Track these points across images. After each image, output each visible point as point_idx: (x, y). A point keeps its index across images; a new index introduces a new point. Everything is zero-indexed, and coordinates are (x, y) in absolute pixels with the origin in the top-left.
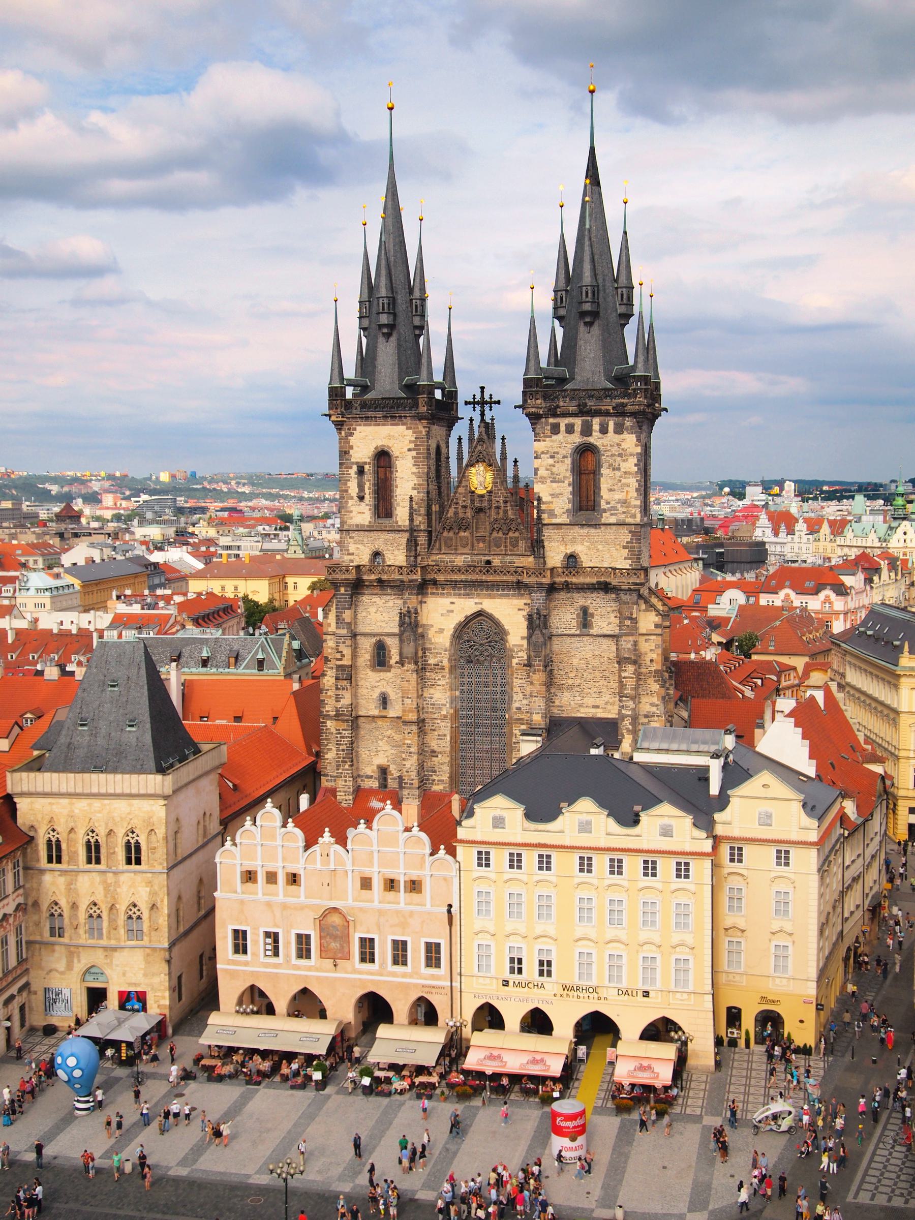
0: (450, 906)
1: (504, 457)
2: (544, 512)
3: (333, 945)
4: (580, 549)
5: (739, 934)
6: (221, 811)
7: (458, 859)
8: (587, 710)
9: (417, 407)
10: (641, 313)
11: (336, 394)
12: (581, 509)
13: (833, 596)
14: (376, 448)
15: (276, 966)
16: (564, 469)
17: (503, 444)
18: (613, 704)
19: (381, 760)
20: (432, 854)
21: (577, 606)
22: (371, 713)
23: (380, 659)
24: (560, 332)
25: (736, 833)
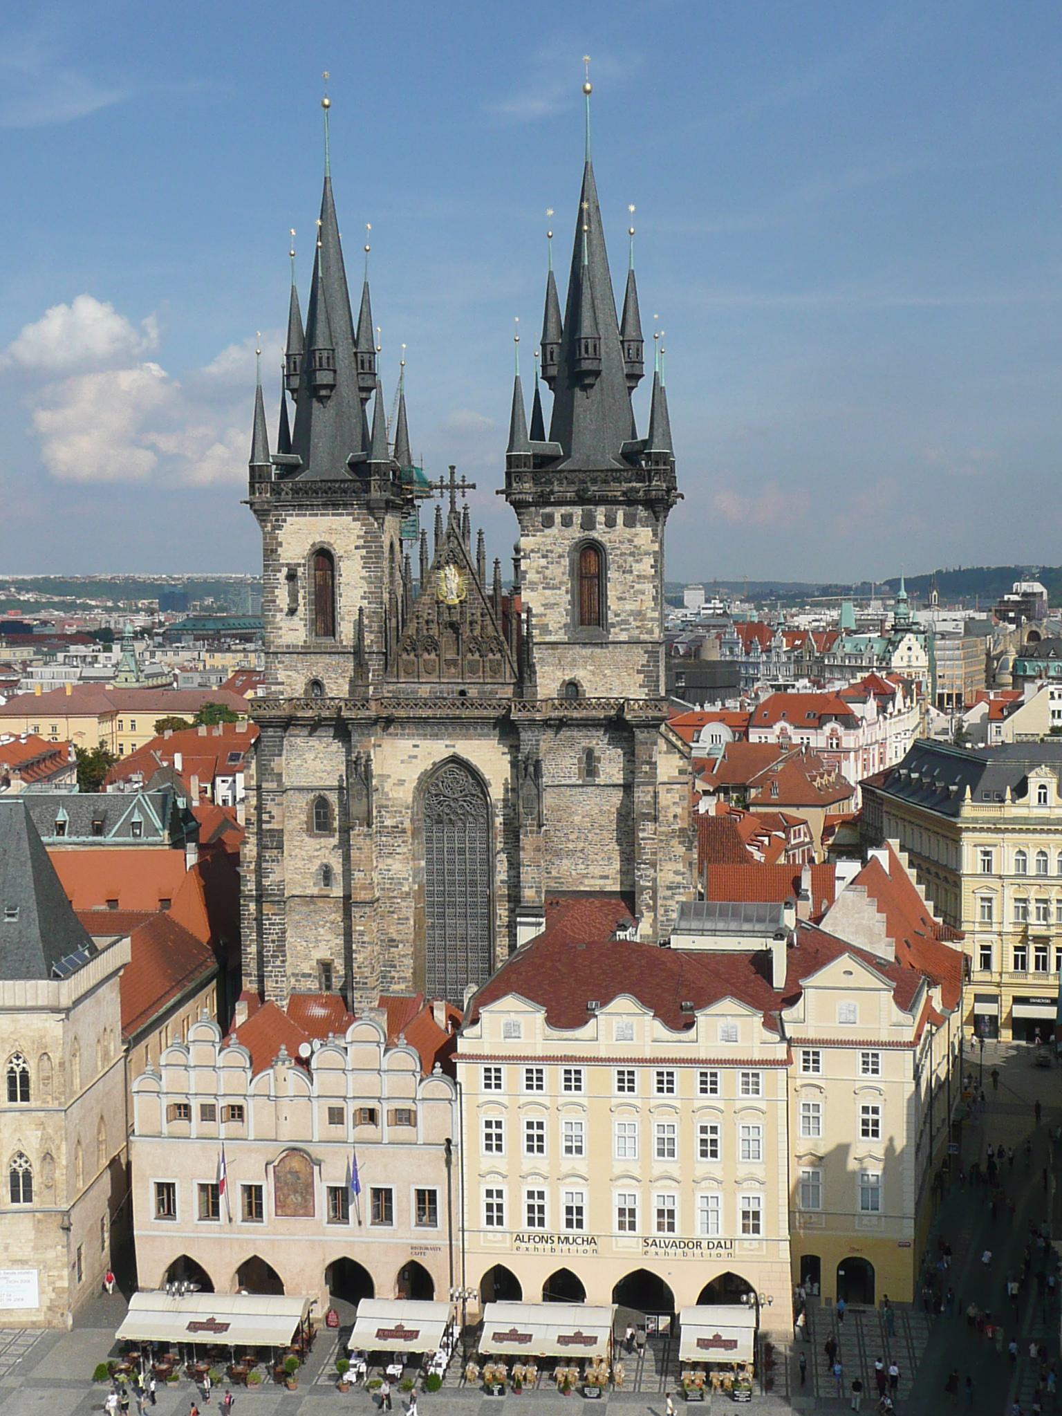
1: (480, 557)
2: (535, 627)
3: (295, 1199)
7: (459, 1079)
8: (592, 882)
9: (368, 491)
11: (257, 475)
12: (582, 624)
13: (841, 730)
14: (313, 545)
16: (560, 571)
17: (480, 540)
19: (323, 953)
21: (580, 747)
22: (308, 892)
23: (320, 820)
25: (811, 1034)
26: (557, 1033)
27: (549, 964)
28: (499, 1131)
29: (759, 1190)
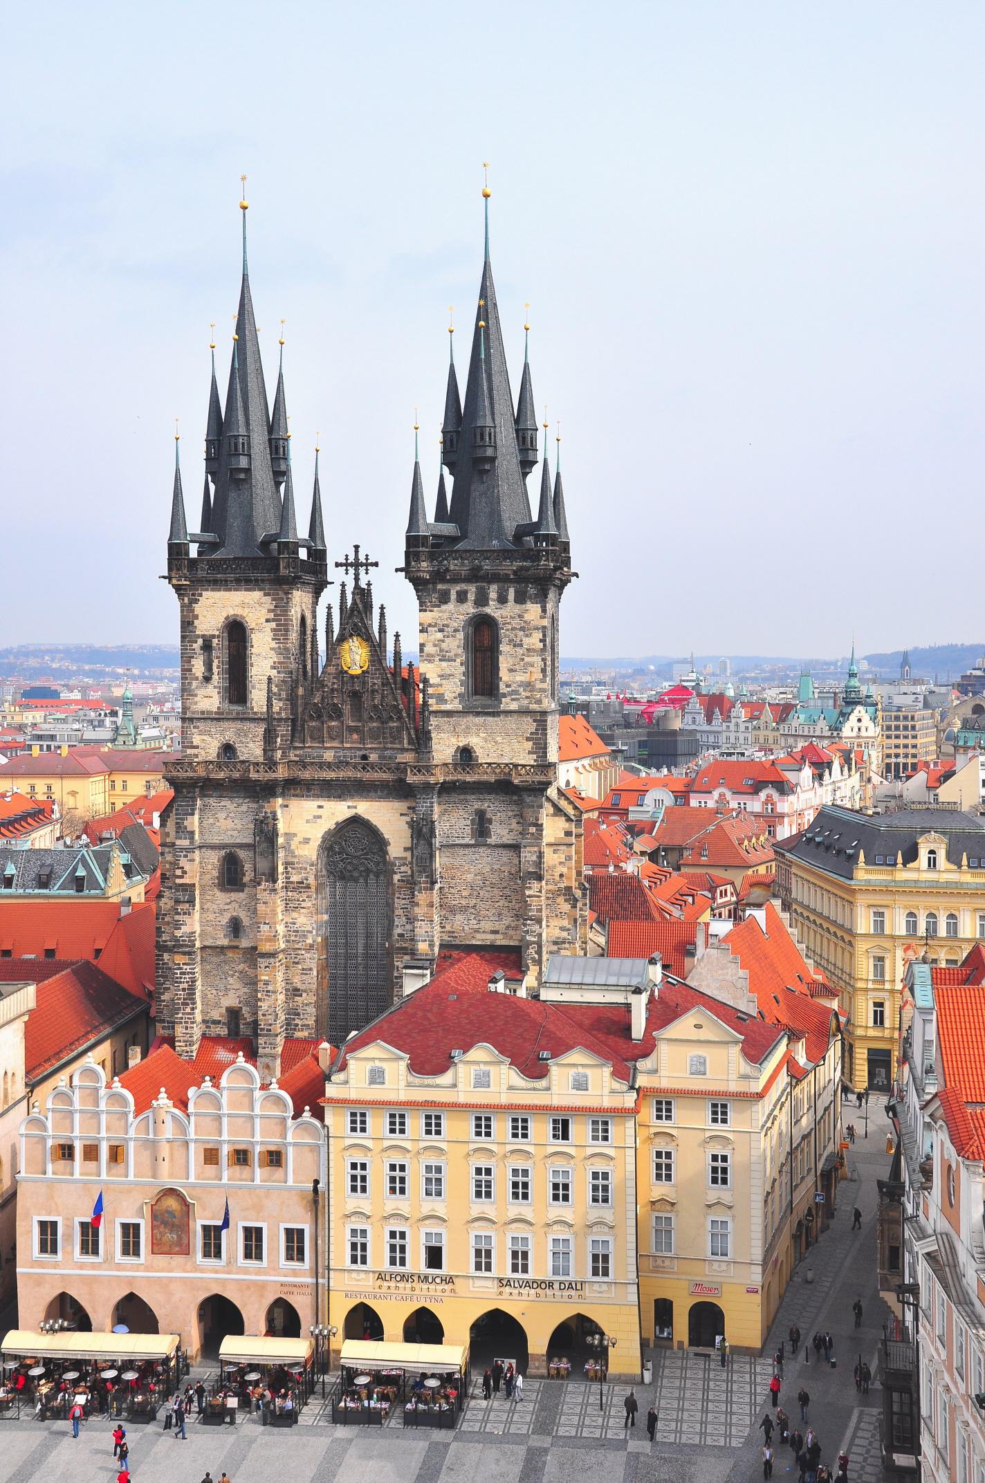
0: (316, 1182)
2: (431, 696)
3: (170, 1237)
4: (475, 741)
5: (669, 1208)
6: (28, 1073)
7: (327, 1122)
9: (278, 569)
10: (545, 460)
11: (176, 552)
12: (476, 693)
13: (776, 796)
14: (227, 618)
15: (93, 1266)
16: (456, 644)
17: (382, 615)
18: (516, 928)
19: (231, 1001)
20: (294, 1118)
21: (471, 809)
22: (219, 943)
23: (231, 875)
24: (449, 481)
25: (665, 1084)
26: (417, 1079)
27: (420, 1014)
28: (363, 1173)
29: (605, 1234)
